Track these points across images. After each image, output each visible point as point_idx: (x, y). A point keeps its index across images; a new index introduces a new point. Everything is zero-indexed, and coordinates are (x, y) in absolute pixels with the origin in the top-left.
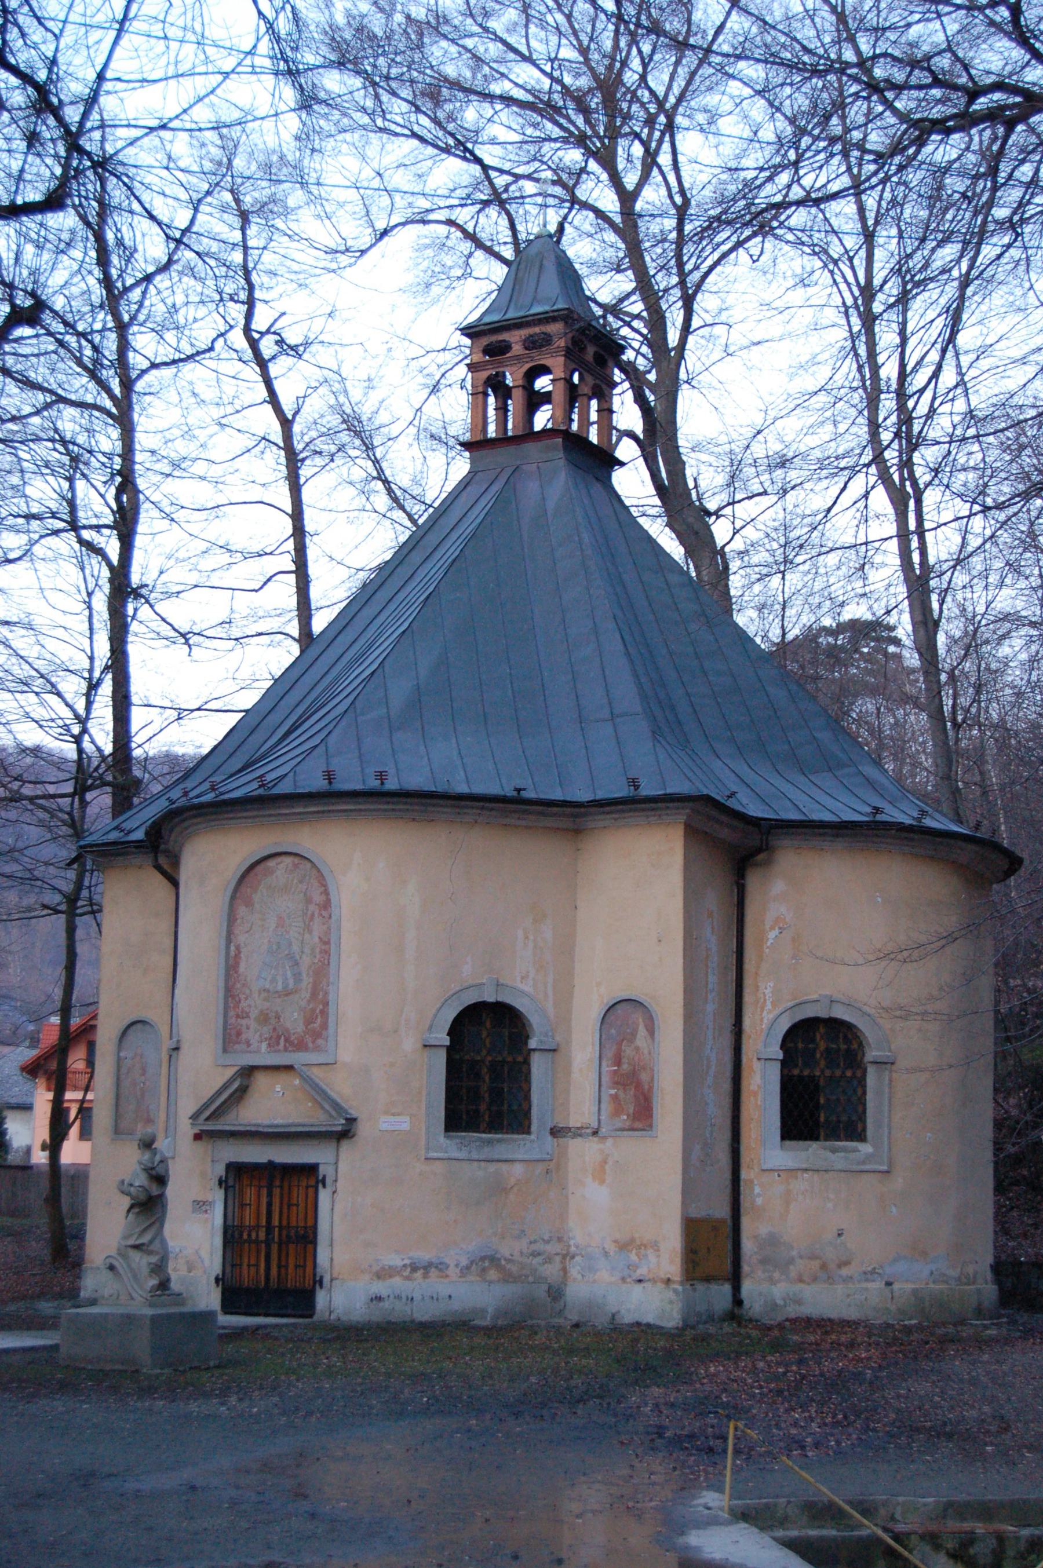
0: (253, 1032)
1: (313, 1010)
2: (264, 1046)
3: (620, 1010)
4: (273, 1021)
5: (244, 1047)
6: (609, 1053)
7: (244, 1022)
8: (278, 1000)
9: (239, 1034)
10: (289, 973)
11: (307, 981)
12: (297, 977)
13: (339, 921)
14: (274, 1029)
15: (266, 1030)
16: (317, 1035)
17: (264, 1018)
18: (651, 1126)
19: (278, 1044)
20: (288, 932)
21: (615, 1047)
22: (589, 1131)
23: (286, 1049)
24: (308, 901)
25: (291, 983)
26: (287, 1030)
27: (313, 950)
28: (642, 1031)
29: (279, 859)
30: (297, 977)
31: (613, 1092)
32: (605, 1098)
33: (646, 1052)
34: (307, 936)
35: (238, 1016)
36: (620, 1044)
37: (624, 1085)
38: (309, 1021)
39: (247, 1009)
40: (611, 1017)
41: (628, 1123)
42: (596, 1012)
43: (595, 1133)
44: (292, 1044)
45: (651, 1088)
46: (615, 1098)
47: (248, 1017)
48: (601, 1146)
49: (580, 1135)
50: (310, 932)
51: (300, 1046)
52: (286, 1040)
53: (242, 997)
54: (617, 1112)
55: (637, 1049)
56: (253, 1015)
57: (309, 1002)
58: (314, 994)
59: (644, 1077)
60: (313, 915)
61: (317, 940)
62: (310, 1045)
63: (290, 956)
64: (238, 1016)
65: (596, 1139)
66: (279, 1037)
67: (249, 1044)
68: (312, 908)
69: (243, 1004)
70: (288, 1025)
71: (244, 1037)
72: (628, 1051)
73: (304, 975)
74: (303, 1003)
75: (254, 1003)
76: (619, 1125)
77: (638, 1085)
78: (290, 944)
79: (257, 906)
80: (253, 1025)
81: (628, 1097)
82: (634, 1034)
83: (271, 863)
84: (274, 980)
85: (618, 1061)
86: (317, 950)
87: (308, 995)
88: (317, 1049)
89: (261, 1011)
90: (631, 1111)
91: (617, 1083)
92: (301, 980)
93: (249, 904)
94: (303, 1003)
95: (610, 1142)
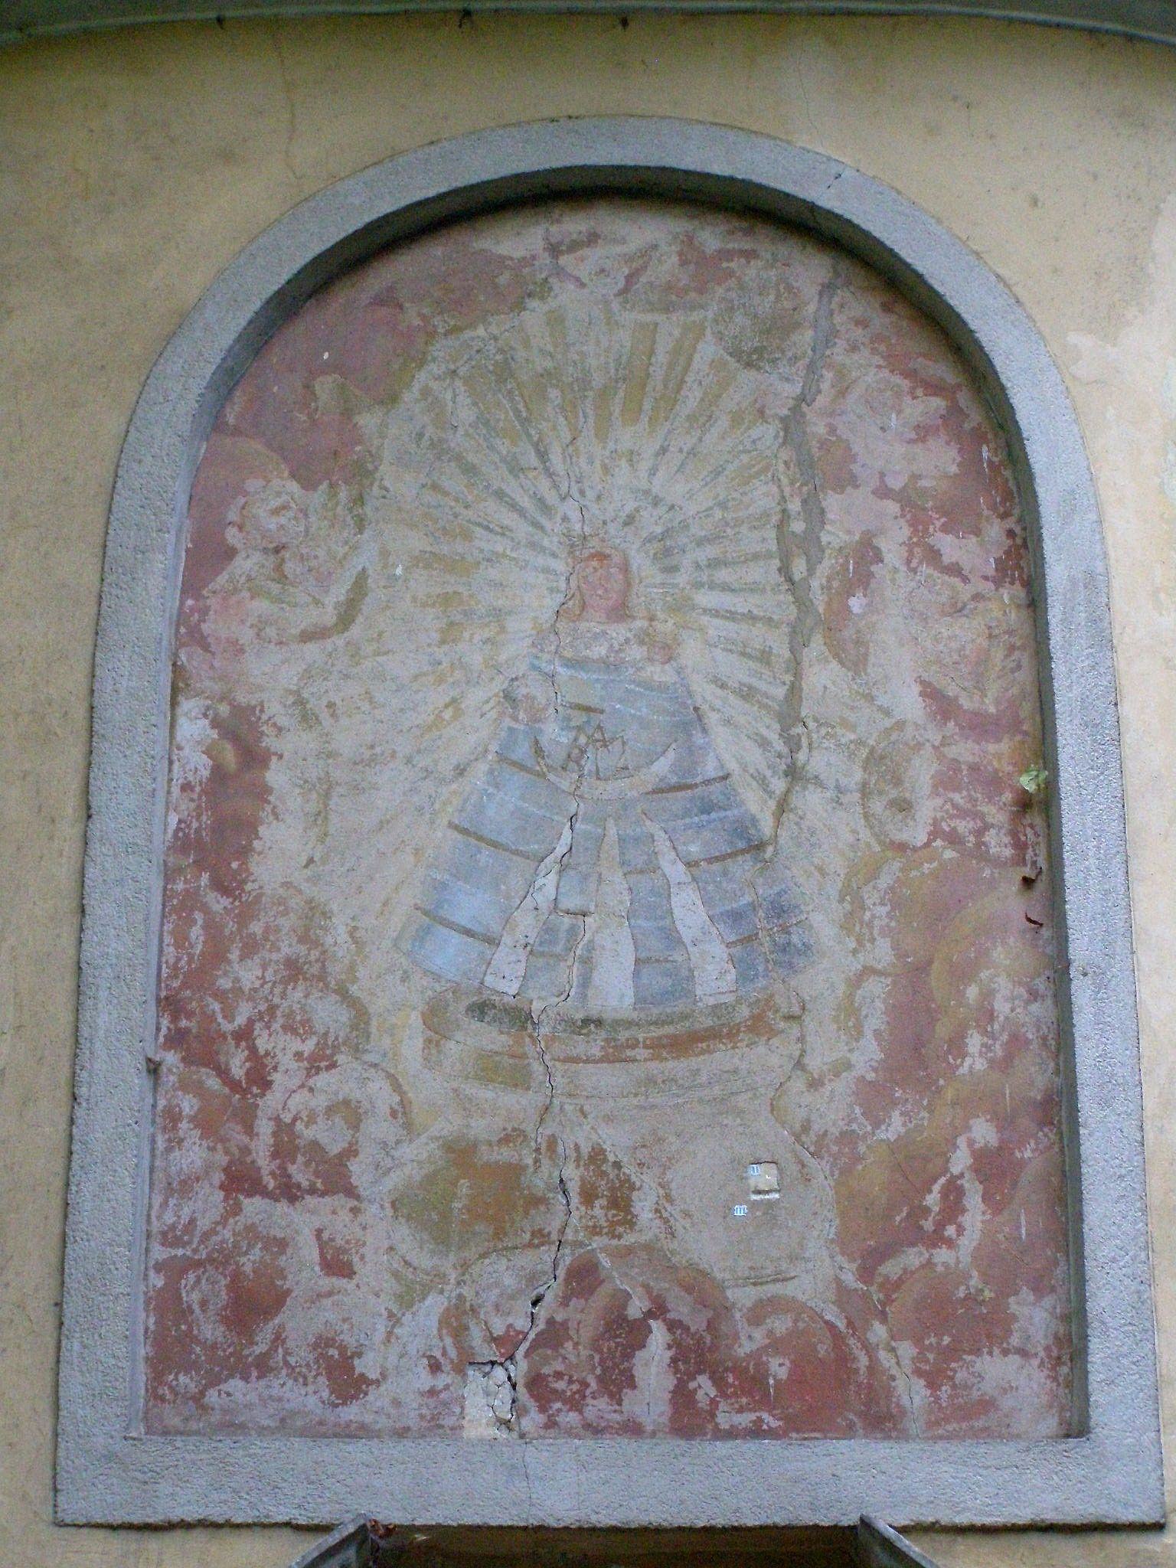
0: (378, 1284)
1: (916, 1166)
2: (483, 1401)
4: (571, 1219)
5: (311, 1398)
7: (302, 1223)
8: (609, 1078)
9: (253, 1304)
10: (689, 912)
11: (843, 965)
12: (767, 935)
13: (1094, 584)
14: (583, 1278)
15: (505, 1285)
16: (960, 1327)
17: (482, 1197)
19: (618, 1380)
20: (668, 651)
23: (688, 1420)
24: (822, 469)
25: (714, 977)
26: (700, 1285)
27: (883, 766)
29: (573, 224)
30: (767, 935)
34: (823, 676)
35: (240, 1181)
38: (893, 1216)
39: (330, 1136)
44: (751, 1384)
47: (335, 1179)
50: (853, 655)
51: (828, 1393)
52: (694, 1356)
53: (283, 1049)
56: (394, 1162)
57: (874, 1098)
58: (916, 1052)
60: (867, 553)
61: (910, 705)
62: (912, 1394)
63: (694, 794)
64: (240, 1181)
66: (624, 1335)
67: (345, 1378)
68: (845, 517)
69: (287, 1096)
70: (705, 1247)
71: (298, 1326)
73: (822, 923)
74: (832, 1109)
75: (404, 1094)
78: (690, 721)
79: (398, 482)
80: (383, 1240)
83: (517, 241)
84: (559, 942)
86: (922, 772)
87: (867, 1055)
88: (970, 1418)
89: (460, 1153)
92: (790, 954)
93: (336, 466)
94: (832, 1109)
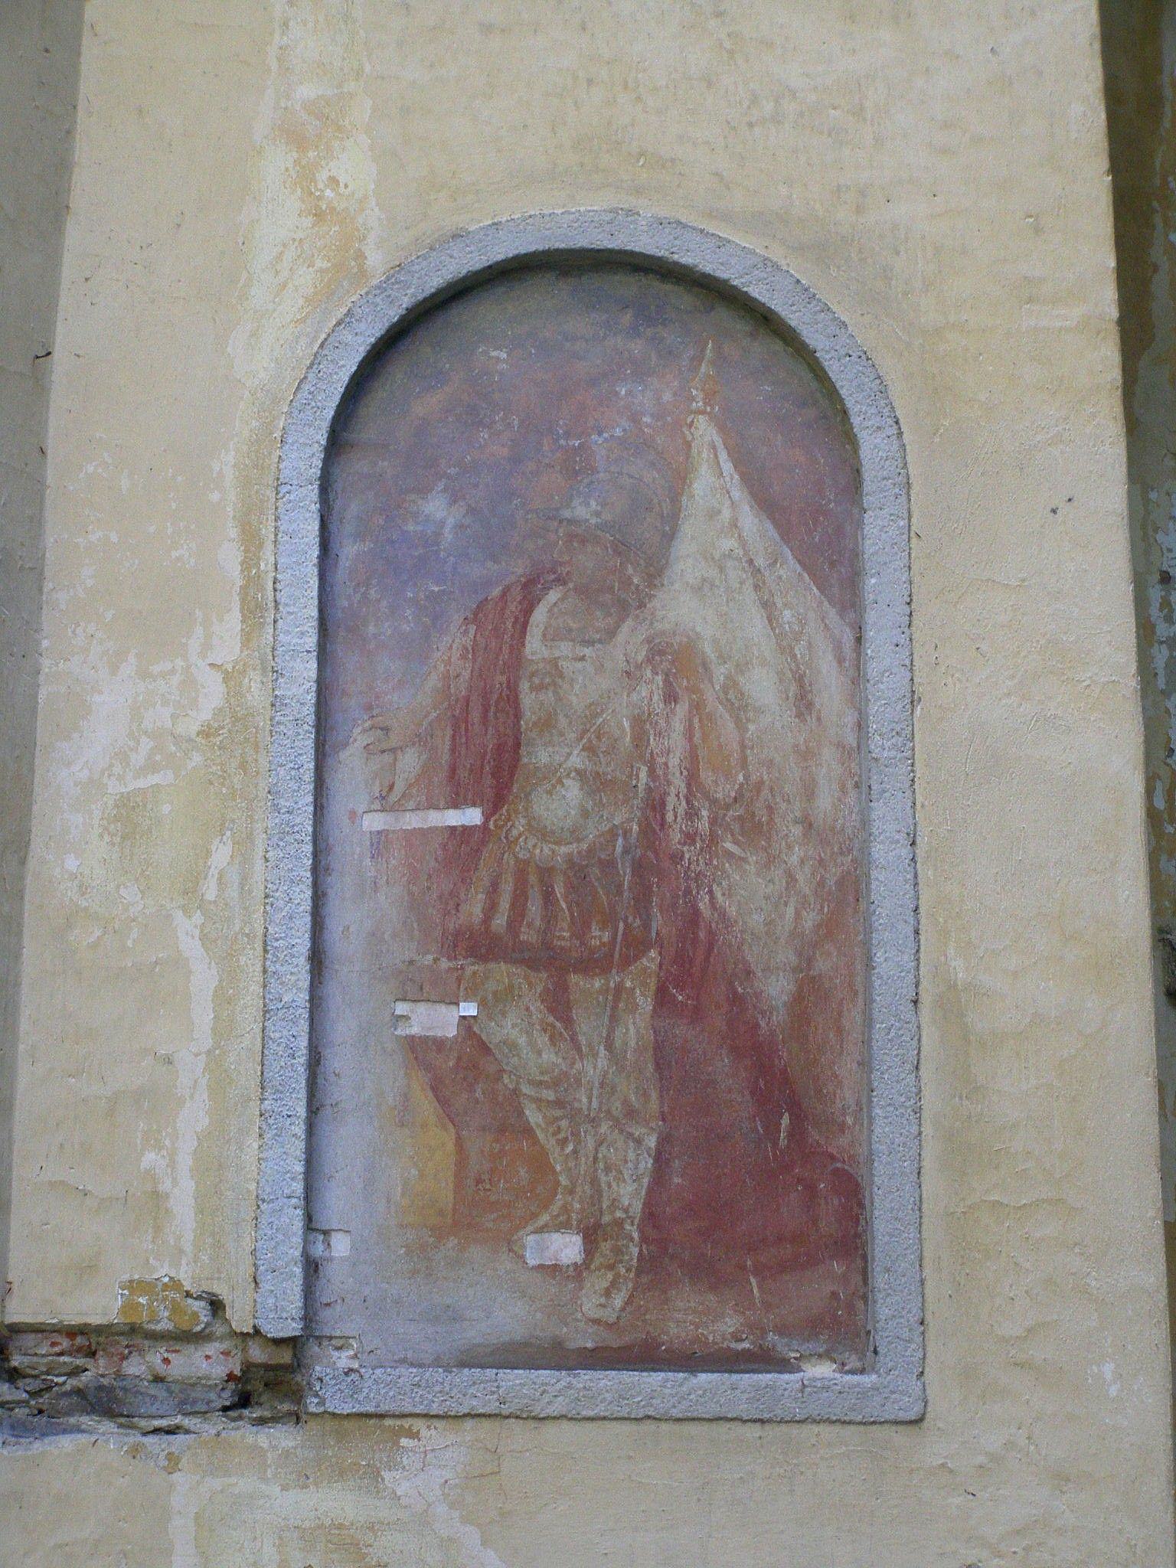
3: (496, 349)
6: (413, 681)
18: (846, 1330)
21: (453, 645)
22: (208, 1364)
28: (718, 514)
31: (440, 1020)
32: (364, 1075)
33: (763, 687)
36: (504, 619)
37: (556, 967)
40: (416, 400)
41: (598, 1304)
42: (274, 338)
43: (269, 1383)
45: (829, 993)
46: (458, 1075)
48: (337, 1502)
49: (106, 1403)
54: (478, 1209)
55: (677, 664)
59: (756, 900)
65: (282, 1438)
72: (582, 674)
76: (509, 1316)
77: (696, 971)
81: (594, 1070)
82: (627, 565)
85: (488, 753)
90: (628, 1194)
91: (478, 945)
95: (427, 1471)
